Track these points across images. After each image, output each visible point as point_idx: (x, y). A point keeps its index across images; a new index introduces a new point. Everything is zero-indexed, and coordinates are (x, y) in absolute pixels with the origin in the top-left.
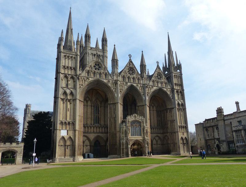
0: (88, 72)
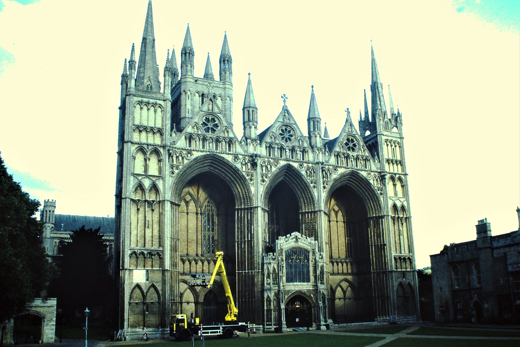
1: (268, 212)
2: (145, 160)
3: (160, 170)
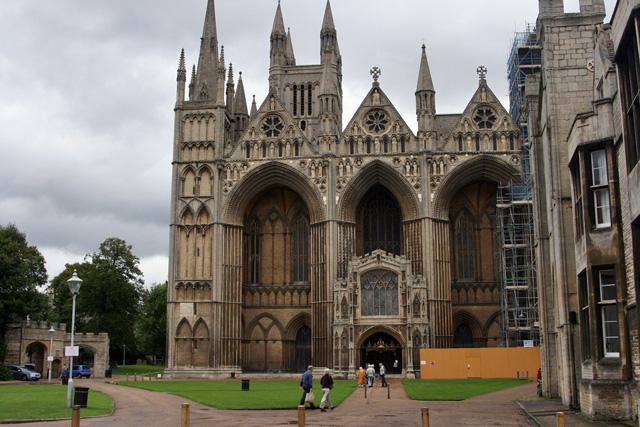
0: (248, 147)
1: (353, 225)
3: (212, 188)
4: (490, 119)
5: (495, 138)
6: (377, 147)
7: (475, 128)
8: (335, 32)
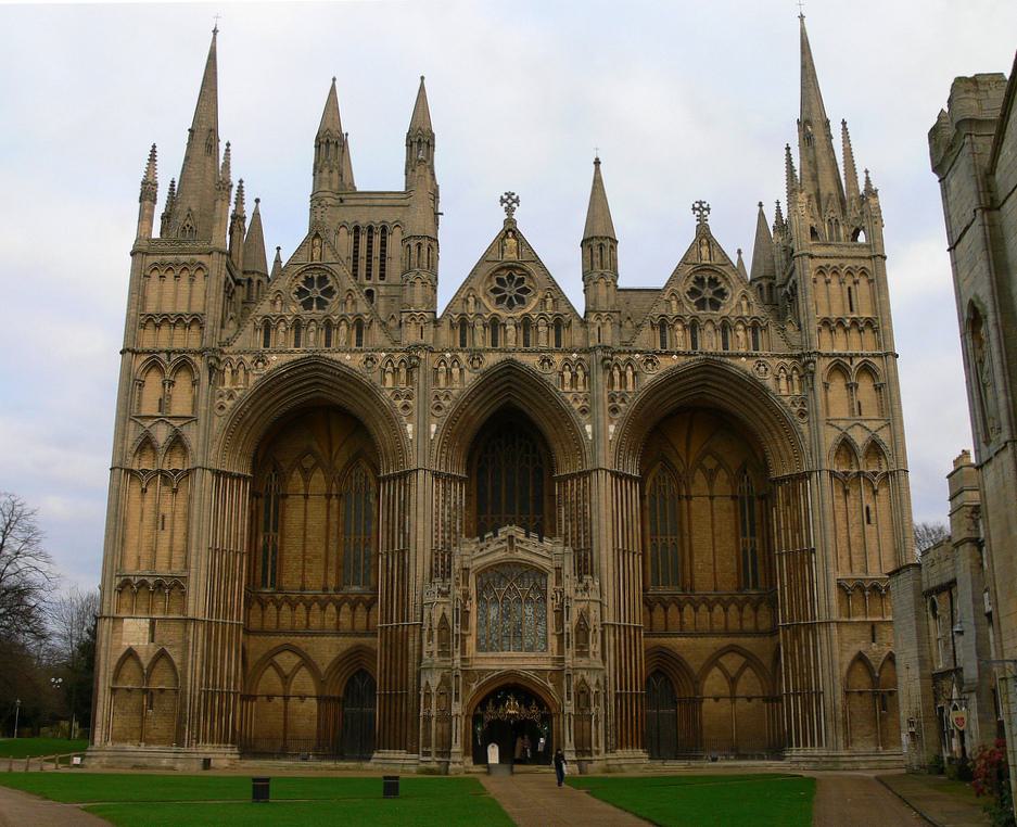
0: (267, 327)
1: (461, 480)
2: (164, 384)
3: (194, 406)
4: (715, 293)
5: (725, 328)
6: (511, 335)
7: (690, 309)
8: (432, 136)
